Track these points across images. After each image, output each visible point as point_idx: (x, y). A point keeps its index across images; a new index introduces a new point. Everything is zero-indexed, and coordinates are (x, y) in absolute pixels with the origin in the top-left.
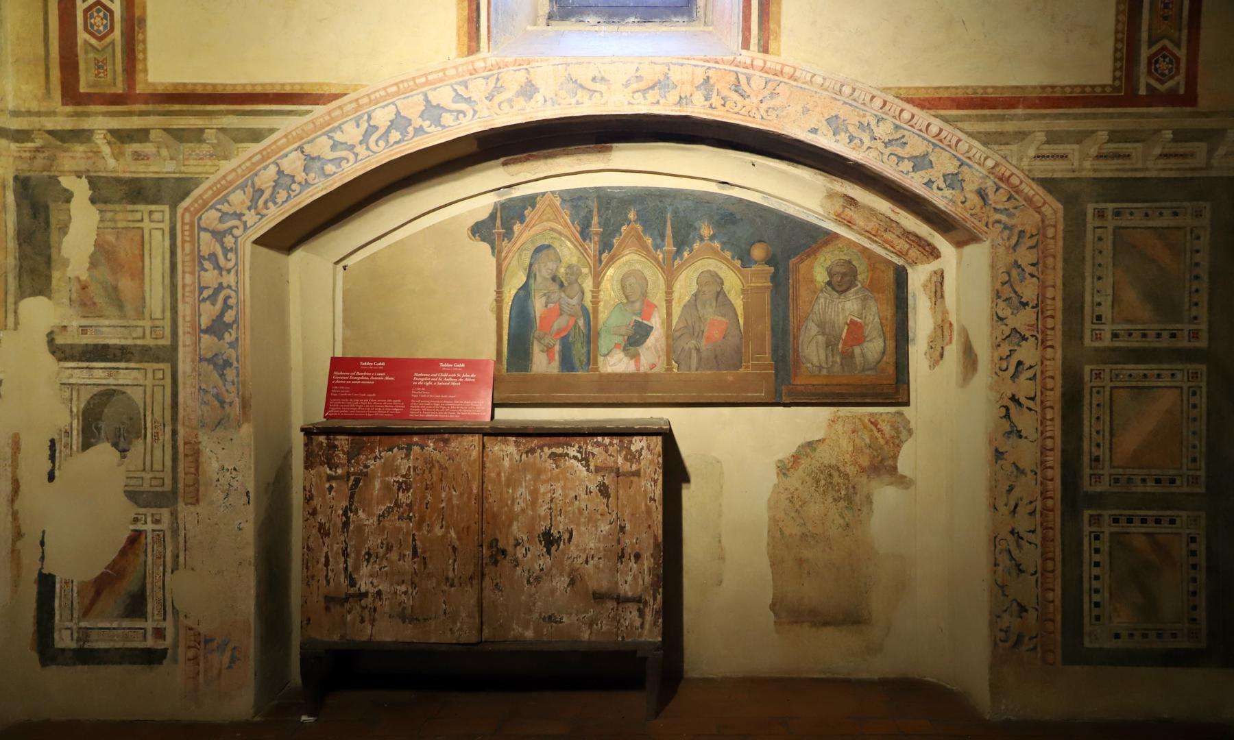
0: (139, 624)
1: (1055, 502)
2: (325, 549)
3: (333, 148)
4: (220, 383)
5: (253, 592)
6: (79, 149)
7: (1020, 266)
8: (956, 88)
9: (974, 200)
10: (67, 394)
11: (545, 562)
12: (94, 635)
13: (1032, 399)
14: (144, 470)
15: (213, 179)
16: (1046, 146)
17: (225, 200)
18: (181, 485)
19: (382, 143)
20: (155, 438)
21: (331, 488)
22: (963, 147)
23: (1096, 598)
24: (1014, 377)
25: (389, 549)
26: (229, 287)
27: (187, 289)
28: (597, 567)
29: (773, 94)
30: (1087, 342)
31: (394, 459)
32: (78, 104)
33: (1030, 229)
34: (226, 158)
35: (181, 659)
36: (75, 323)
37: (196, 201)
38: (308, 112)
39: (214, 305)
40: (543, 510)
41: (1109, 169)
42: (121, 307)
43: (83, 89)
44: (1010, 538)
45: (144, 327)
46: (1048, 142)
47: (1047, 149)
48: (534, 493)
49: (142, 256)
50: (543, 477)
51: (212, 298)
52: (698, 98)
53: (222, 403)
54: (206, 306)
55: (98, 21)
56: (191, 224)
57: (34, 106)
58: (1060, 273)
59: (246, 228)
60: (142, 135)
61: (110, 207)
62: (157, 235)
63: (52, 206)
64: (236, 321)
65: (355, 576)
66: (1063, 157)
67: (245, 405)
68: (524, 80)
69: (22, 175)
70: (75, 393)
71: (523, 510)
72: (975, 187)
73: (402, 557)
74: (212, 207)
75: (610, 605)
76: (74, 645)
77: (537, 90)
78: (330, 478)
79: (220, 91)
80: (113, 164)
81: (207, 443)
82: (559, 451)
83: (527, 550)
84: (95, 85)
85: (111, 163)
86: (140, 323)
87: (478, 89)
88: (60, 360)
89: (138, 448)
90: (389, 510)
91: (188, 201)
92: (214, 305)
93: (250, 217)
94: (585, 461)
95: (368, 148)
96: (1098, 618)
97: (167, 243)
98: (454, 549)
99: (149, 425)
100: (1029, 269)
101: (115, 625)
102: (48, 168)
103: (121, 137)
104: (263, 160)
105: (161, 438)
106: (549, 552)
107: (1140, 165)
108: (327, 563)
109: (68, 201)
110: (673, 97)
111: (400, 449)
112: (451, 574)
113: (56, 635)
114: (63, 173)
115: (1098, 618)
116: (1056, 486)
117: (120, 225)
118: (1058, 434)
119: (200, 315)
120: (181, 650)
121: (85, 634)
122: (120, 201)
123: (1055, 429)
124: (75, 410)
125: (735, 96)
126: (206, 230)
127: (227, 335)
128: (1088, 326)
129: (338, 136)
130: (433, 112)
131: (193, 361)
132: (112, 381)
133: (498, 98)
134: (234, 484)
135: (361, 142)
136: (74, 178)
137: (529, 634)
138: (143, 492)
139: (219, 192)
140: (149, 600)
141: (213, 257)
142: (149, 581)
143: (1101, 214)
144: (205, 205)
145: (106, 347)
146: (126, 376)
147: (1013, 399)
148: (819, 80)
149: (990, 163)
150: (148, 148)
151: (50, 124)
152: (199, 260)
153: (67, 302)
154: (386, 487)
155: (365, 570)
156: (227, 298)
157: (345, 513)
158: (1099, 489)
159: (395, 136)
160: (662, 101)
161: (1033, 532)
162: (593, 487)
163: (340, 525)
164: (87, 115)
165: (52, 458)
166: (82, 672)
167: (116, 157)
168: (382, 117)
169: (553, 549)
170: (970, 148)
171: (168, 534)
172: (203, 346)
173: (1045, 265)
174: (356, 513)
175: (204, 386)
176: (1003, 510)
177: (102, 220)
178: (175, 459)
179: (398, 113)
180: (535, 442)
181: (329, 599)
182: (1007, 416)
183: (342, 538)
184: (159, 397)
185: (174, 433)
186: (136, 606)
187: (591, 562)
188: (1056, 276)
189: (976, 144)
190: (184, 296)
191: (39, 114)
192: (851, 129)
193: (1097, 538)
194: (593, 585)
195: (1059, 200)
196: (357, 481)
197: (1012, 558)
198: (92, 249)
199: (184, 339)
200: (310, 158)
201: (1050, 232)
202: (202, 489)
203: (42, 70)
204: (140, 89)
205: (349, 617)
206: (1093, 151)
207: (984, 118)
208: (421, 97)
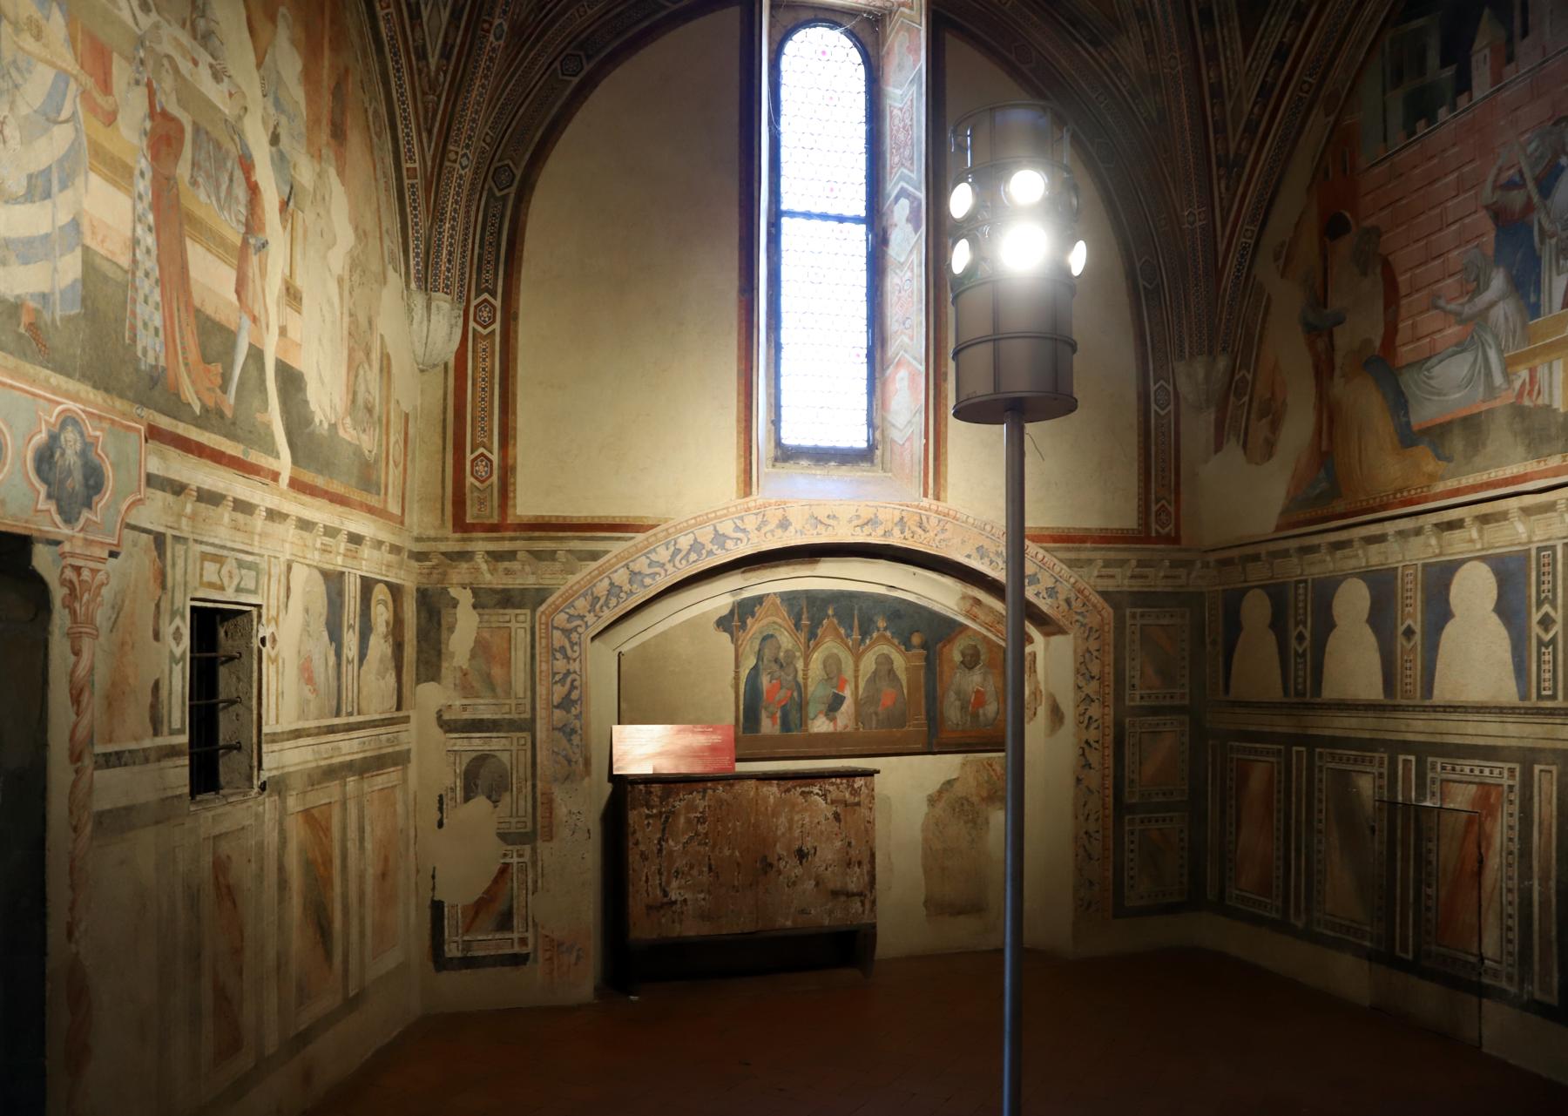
0: (508, 935)
1: (1110, 812)
2: (646, 870)
3: (650, 566)
4: (568, 746)
6: (464, 565)
7: (1090, 652)
8: (1053, 528)
9: (1064, 606)
10: (452, 758)
11: (798, 871)
13: (1097, 742)
14: (511, 816)
15: (563, 589)
17: (572, 605)
18: (539, 827)
19: (684, 562)
20: (519, 790)
21: (649, 824)
22: (1057, 569)
23: (1132, 873)
24: (1087, 727)
25: (692, 867)
26: (575, 672)
27: (543, 674)
28: (833, 872)
29: (944, 530)
30: (1127, 703)
31: (694, 800)
32: (465, 531)
33: (1096, 627)
34: (573, 573)
35: (541, 960)
36: (458, 703)
37: (550, 606)
38: (632, 538)
39: (563, 686)
40: (797, 833)
41: (1137, 586)
44: (1084, 836)
45: (510, 705)
46: (1104, 567)
47: (1105, 571)
48: (791, 821)
49: (510, 648)
50: (797, 809)
51: (562, 681)
52: (897, 531)
53: (569, 762)
54: (558, 688)
55: (481, 469)
56: (547, 624)
57: (432, 533)
58: (1112, 656)
59: (587, 627)
60: (511, 555)
61: (487, 611)
63: (443, 612)
64: (580, 698)
65: (667, 889)
66: (1112, 577)
68: (781, 518)
69: (422, 587)
70: (458, 759)
71: (783, 834)
72: (1064, 597)
73: (701, 873)
74: (562, 611)
75: (843, 899)
76: (459, 955)
77: (790, 524)
78: (648, 816)
79: (568, 521)
80: (491, 578)
81: (559, 794)
82: (807, 789)
83: (787, 863)
84: (478, 517)
85: (488, 577)
86: (508, 701)
87: (751, 522)
88: (446, 732)
89: (506, 799)
90: (691, 838)
91: (544, 606)
92: (563, 686)
93: (590, 618)
94: (824, 796)
95: (674, 566)
96: (1132, 886)
98: (738, 864)
99: (514, 781)
100: (1095, 654)
102: (441, 581)
103: (496, 557)
104: (600, 574)
105: (524, 791)
106: (801, 863)
107: (1153, 583)
108: (647, 881)
109: (455, 607)
110: (880, 531)
111: (698, 792)
112: (736, 883)
113: (446, 948)
115: (1132, 886)
116: (1110, 800)
117: (494, 625)
118: (1111, 765)
119: (553, 694)
120: (540, 953)
121: (467, 945)
122: (494, 606)
123: (1110, 762)
124: (458, 771)
125: (920, 531)
126: (557, 628)
128: (1128, 692)
129: (653, 557)
130: (720, 539)
131: (548, 730)
133: (764, 530)
134: (579, 823)
135: (669, 561)
136: (460, 589)
137: (789, 923)
138: (510, 833)
139: (566, 600)
141: (562, 649)
142: (515, 902)
143: (1133, 616)
146: (496, 743)
147: (1087, 742)
148: (971, 520)
149: (1072, 580)
150: (516, 565)
151: (443, 547)
152: (552, 652)
153: (453, 686)
154: (689, 821)
155: (675, 884)
157: (659, 843)
158: (1134, 801)
159: (693, 556)
160: (873, 534)
161: (1097, 832)
162: (830, 815)
163: (656, 851)
164: (471, 540)
165: (441, 809)
166: (466, 976)
167: (492, 572)
168: (685, 542)
169: (804, 861)
170: (1062, 569)
171: (529, 864)
172: (555, 718)
173: (1104, 651)
174: (667, 841)
175: (556, 750)
176: (1082, 818)
177: (481, 622)
179: (695, 539)
180: (790, 784)
181: (649, 908)
182: (1083, 754)
183: (657, 861)
184: (522, 759)
185: (534, 786)
186: (505, 922)
187: (829, 869)
188: (1110, 658)
189: (1064, 567)
190: (540, 679)
191: (435, 539)
192: (991, 555)
193: (1132, 833)
194: (831, 886)
195: (1111, 606)
196: (667, 818)
197: (1086, 851)
198: (472, 645)
199: (541, 713)
200: (633, 574)
201: (1106, 628)
202: (554, 829)
203: (439, 506)
205: (663, 920)
206: (1129, 573)
207: (1068, 550)
208: (712, 528)
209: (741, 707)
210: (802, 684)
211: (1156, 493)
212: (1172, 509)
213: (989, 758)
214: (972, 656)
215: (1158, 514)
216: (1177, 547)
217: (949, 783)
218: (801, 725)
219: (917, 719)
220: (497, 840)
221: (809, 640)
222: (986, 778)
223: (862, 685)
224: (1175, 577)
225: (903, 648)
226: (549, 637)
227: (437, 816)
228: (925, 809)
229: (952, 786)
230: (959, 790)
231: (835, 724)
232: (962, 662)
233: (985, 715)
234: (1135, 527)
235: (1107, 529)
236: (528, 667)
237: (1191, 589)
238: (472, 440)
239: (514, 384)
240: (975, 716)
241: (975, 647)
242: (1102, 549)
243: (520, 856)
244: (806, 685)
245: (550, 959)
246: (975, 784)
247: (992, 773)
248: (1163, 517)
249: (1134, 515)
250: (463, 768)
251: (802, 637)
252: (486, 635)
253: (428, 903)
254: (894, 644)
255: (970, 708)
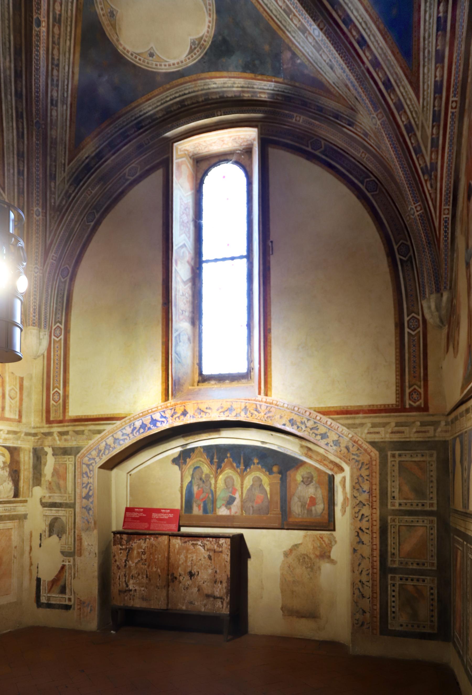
0: (64, 596)
1: (377, 570)
2: (119, 574)
3: (123, 435)
4: (88, 515)
5: (97, 587)
6: (50, 438)
7: (362, 476)
8: (337, 407)
9: (344, 450)
10: (45, 519)
11: (189, 582)
12: (51, 599)
13: (368, 529)
14: (66, 544)
15: (87, 447)
16: (372, 429)
17: (90, 454)
18: (76, 550)
19: (138, 433)
21: (121, 553)
22: (340, 430)
23: (393, 610)
24: (361, 520)
25: (139, 575)
26: (91, 483)
28: (207, 585)
29: (269, 411)
30: (389, 507)
31: (141, 543)
33: (366, 462)
34: (91, 440)
35: (76, 608)
36: (47, 495)
37: (82, 454)
39: (86, 489)
40: (189, 564)
41: (396, 438)
42: (60, 490)
43: (51, 419)
44: (359, 584)
46: (372, 427)
47: (372, 430)
48: (186, 557)
49: (66, 473)
50: (189, 552)
51: (86, 487)
52: (243, 414)
53: (88, 522)
54: (84, 490)
55: (56, 397)
57: (38, 425)
58: (378, 480)
59: (96, 463)
60: (66, 433)
61: (58, 457)
62: (71, 466)
63: (42, 457)
64: (93, 494)
65: (128, 584)
66: (378, 433)
67: (95, 523)
68: (183, 410)
71: (182, 563)
72: (345, 445)
73: (143, 578)
74: (86, 456)
75: (212, 599)
76: (46, 602)
77: (188, 413)
78: (121, 549)
80: (59, 443)
81: (84, 536)
82: (195, 542)
83: (184, 578)
85: (58, 442)
86: (65, 495)
87: (168, 413)
89: (64, 537)
90: (139, 561)
92: (86, 489)
93: (97, 459)
94: (204, 546)
95: (133, 435)
96: (394, 618)
97: (73, 468)
98: (159, 576)
100: (366, 478)
101: (57, 596)
102: (41, 445)
103: (61, 434)
104: (102, 440)
106: (191, 579)
107: (408, 436)
108: (119, 579)
109: (46, 455)
110: (234, 414)
111: (143, 540)
112: (158, 585)
113: (41, 598)
114: (45, 446)
115: (394, 618)
116: (377, 564)
117: (61, 462)
118: (378, 543)
120: (76, 606)
121: (49, 598)
122: (60, 455)
123: (377, 541)
125: (255, 413)
126: (84, 464)
127: (90, 499)
128: (389, 501)
129: (124, 431)
130: (154, 422)
132: (57, 514)
133: (175, 416)
134: (92, 550)
135: (131, 433)
136: (48, 448)
137: (184, 608)
140: (67, 588)
141: (86, 473)
142: (67, 582)
143: (393, 456)
144: (84, 456)
145: (56, 503)
146: (61, 513)
147: (360, 529)
148: (286, 405)
149: (350, 436)
150: (68, 437)
151: (43, 431)
152: (82, 474)
154: (138, 553)
155: (131, 582)
156: (90, 487)
157: (125, 562)
158: (394, 566)
159: (142, 430)
160: (230, 415)
161: (368, 582)
162: (206, 556)
163: (123, 565)
164: (52, 427)
165: (41, 539)
166: (48, 611)
167: (60, 440)
168: (138, 424)
169: (192, 578)
170: (343, 430)
173: (372, 476)
174: (129, 562)
175: (83, 516)
176: (357, 572)
177: (55, 461)
178: (74, 541)
179: (143, 423)
180: (187, 539)
181: (120, 591)
182: (358, 535)
183: (124, 570)
184: (70, 520)
185: (75, 532)
186: (63, 590)
187: (205, 583)
188: (376, 480)
189: (345, 428)
191: (39, 428)
192: (298, 424)
193: (394, 586)
194: (206, 592)
195: (377, 450)
196: (129, 551)
197: (360, 592)
198: (52, 471)
199: (78, 501)
200: (115, 439)
201: (374, 463)
202: (82, 551)
204: (67, 418)
205: (126, 598)
206: (390, 431)
207: (347, 418)
208: (150, 417)
209: (184, 501)
210: (214, 491)
211: (409, 382)
212: (422, 391)
213: (321, 534)
214: (308, 478)
215: (410, 394)
216: (425, 413)
217: (296, 545)
218: (213, 511)
219: (275, 511)
220: (60, 554)
221: (217, 469)
222: (319, 545)
223: (245, 491)
224: (425, 432)
225: (268, 473)
226: (81, 467)
227: (39, 542)
228: (282, 558)
229: (298, 547)
230: (302, 550)
231: (230, 512)
232: (302, 481)
233: (316, 510)
234: (394, 402)
235: (373, 405)
236: (73, 481)
237: (437, 439)
238: (53, 385)
239: (69, 360)
240: (310, 511)
241: (310, 473)
242: (370, 417)
243: (69, 562)
244: (215, 491)
245: (80, 609)
246: (312, 548)
247: (323, 543)
248: (415, 396)
249: (394, 396)
250: (49, 522)
251: (214, 467)
252: (58, 467)
253: (35, 578)
254: (237, 472)
255: (307, 506)
